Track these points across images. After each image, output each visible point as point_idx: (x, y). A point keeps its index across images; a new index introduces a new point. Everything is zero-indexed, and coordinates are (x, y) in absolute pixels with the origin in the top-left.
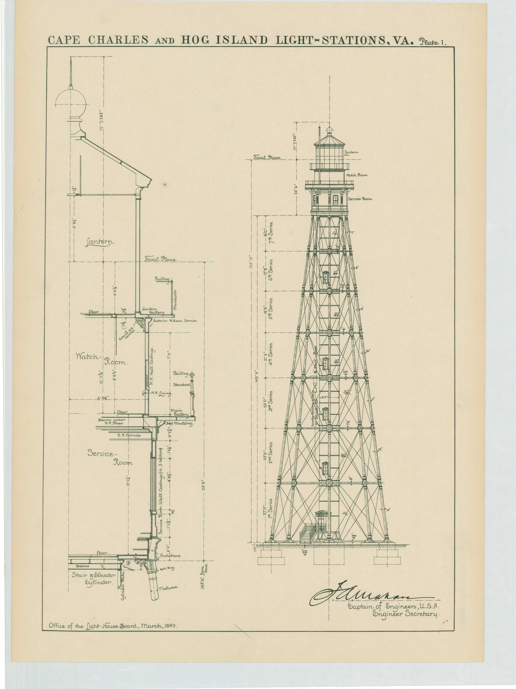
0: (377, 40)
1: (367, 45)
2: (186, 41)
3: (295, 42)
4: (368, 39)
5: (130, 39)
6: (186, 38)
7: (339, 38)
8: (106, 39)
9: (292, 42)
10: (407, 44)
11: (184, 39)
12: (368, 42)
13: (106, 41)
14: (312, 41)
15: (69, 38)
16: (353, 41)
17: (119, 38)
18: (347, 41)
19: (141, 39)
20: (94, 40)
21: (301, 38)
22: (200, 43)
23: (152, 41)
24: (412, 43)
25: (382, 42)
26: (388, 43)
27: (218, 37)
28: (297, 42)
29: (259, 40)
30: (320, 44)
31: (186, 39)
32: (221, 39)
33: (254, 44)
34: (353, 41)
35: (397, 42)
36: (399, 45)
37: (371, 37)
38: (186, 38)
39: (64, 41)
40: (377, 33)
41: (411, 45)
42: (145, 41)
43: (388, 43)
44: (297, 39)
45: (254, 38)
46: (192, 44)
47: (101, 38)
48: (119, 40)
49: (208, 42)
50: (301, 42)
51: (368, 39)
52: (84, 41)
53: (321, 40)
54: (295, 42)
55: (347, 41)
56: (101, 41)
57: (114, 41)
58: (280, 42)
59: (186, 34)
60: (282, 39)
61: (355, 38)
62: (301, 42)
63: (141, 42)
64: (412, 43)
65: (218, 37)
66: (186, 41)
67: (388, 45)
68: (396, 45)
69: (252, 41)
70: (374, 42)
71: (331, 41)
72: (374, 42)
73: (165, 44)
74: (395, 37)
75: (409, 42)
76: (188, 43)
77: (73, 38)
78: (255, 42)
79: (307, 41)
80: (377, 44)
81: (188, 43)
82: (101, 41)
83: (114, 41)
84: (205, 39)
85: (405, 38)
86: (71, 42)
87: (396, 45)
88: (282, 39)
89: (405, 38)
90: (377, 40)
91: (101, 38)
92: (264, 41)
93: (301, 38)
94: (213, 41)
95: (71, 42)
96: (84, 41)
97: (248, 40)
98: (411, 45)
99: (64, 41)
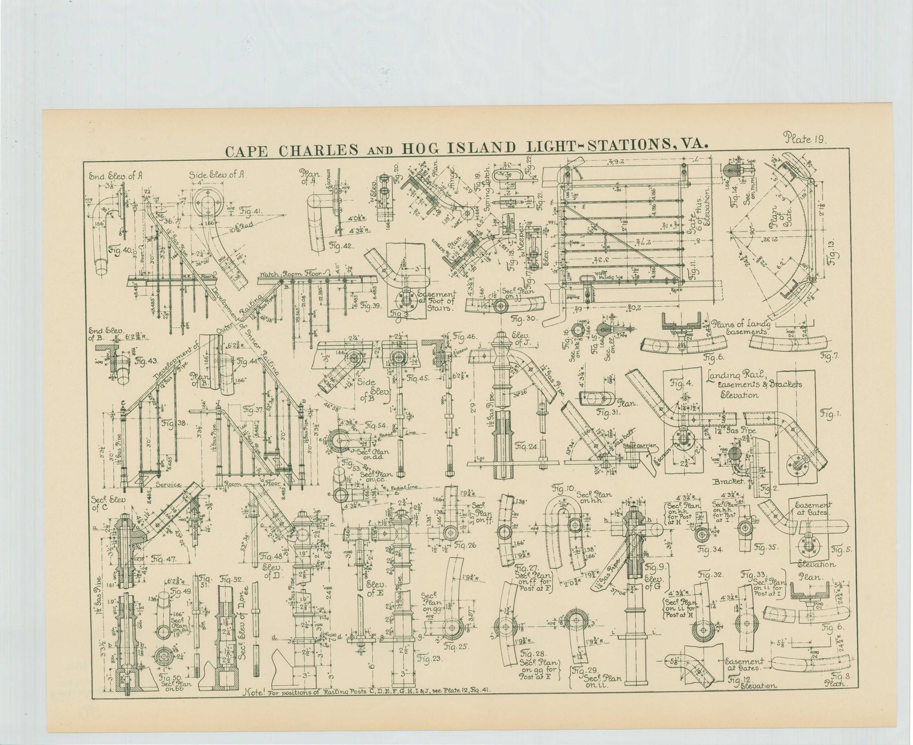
0: (660, 143)
1: (646, 150)
2: (408, 151)
3: (552, 149)
4: (648, 142)
5: (335, 149)
6: (408, 146)
7: (610, 142)
8: (303, 150)
9: (549, 149)
10: (700, 147)
11: (405, 149)
12: (648, 146)
13: (302, 153)
14: (575, 147)
15: (252, 149)
16: (629, 146)
17: (319, 148)
18: (620, 146)
19: (348, 149)
20: (287, 152)
21: (560, 144)
22: (427, 152)
23: (363, 151)
24: (706, 146)
25: (666, 146)
26: (675, 147)
27: (451, 144)
28: (555, 149)
29: (504, 148)
30: (585, 150)
31: (408, 149)
32: (455, 147)
33: (498, 153)
34: (629, 146)
35: (687, 146)
36: (689, 148)
37: (652, 140)
38: (408, 146)
39: (246, 153)
40: (660, 135)
41: (705, 149)
42: (353, 152)
43: (675, 147)
44: (555, 145)
45: (498, 145)
46: (417, 154)
47: (296, 149)
48: (319, 150)
49: (437, 151)
50: (560, 148)
51: (648, 142)
52: (273, 152)
53: (586, 145)
54: (552, 149)
55: (620, 146)
56: (296, 153)
57: (313, 152)
58: (532, 149)
59: (408, 142)
60: (534, 146)
61: (631, 142)
62: (560, 148)
63: (348, 153)
64: (706, 146)
65: (451, 144)
66: (408, 151)
67: (672, 149)
68: (686, 149)
69: (496, 149)
70: (656, 146)
71: (599, 147)
72: (656, 146)
73: (380, 155)
74: (683, 139)
75: (702, 145)
76: (411, 152)
77: (258, 149)
78: (500, 150)
79: (567, 147)
80: (660, 146)
81: (411, 152)
82: (296, 153)
83: (313, 152)
84: (433, 148)
85: (697, 140)
86: (255, 154)
87: (684, 148)
88: (534, 146)
89: (697, 140)
90: (660, 143)
91: (296, 149)
92: (511, 149)
93: (560, 144)
94: (444, 150)
95: (255, 154)
96: (273, 152)
97: (490, 147)
98: (705, 149)
99: (246, 153)
